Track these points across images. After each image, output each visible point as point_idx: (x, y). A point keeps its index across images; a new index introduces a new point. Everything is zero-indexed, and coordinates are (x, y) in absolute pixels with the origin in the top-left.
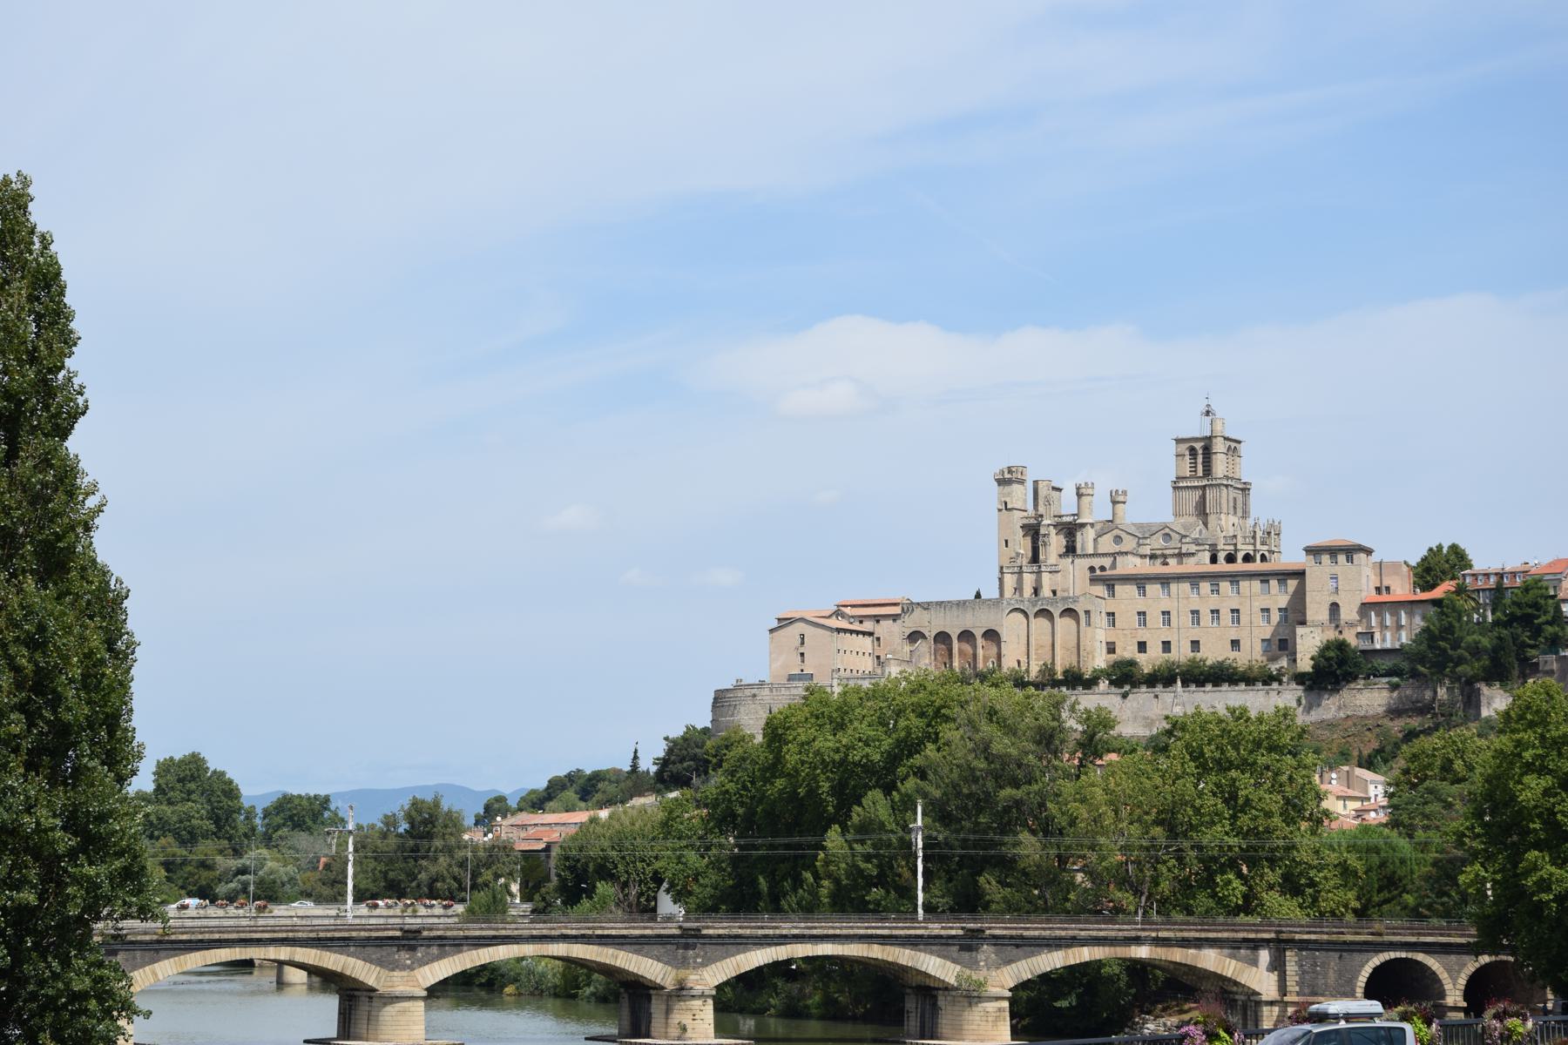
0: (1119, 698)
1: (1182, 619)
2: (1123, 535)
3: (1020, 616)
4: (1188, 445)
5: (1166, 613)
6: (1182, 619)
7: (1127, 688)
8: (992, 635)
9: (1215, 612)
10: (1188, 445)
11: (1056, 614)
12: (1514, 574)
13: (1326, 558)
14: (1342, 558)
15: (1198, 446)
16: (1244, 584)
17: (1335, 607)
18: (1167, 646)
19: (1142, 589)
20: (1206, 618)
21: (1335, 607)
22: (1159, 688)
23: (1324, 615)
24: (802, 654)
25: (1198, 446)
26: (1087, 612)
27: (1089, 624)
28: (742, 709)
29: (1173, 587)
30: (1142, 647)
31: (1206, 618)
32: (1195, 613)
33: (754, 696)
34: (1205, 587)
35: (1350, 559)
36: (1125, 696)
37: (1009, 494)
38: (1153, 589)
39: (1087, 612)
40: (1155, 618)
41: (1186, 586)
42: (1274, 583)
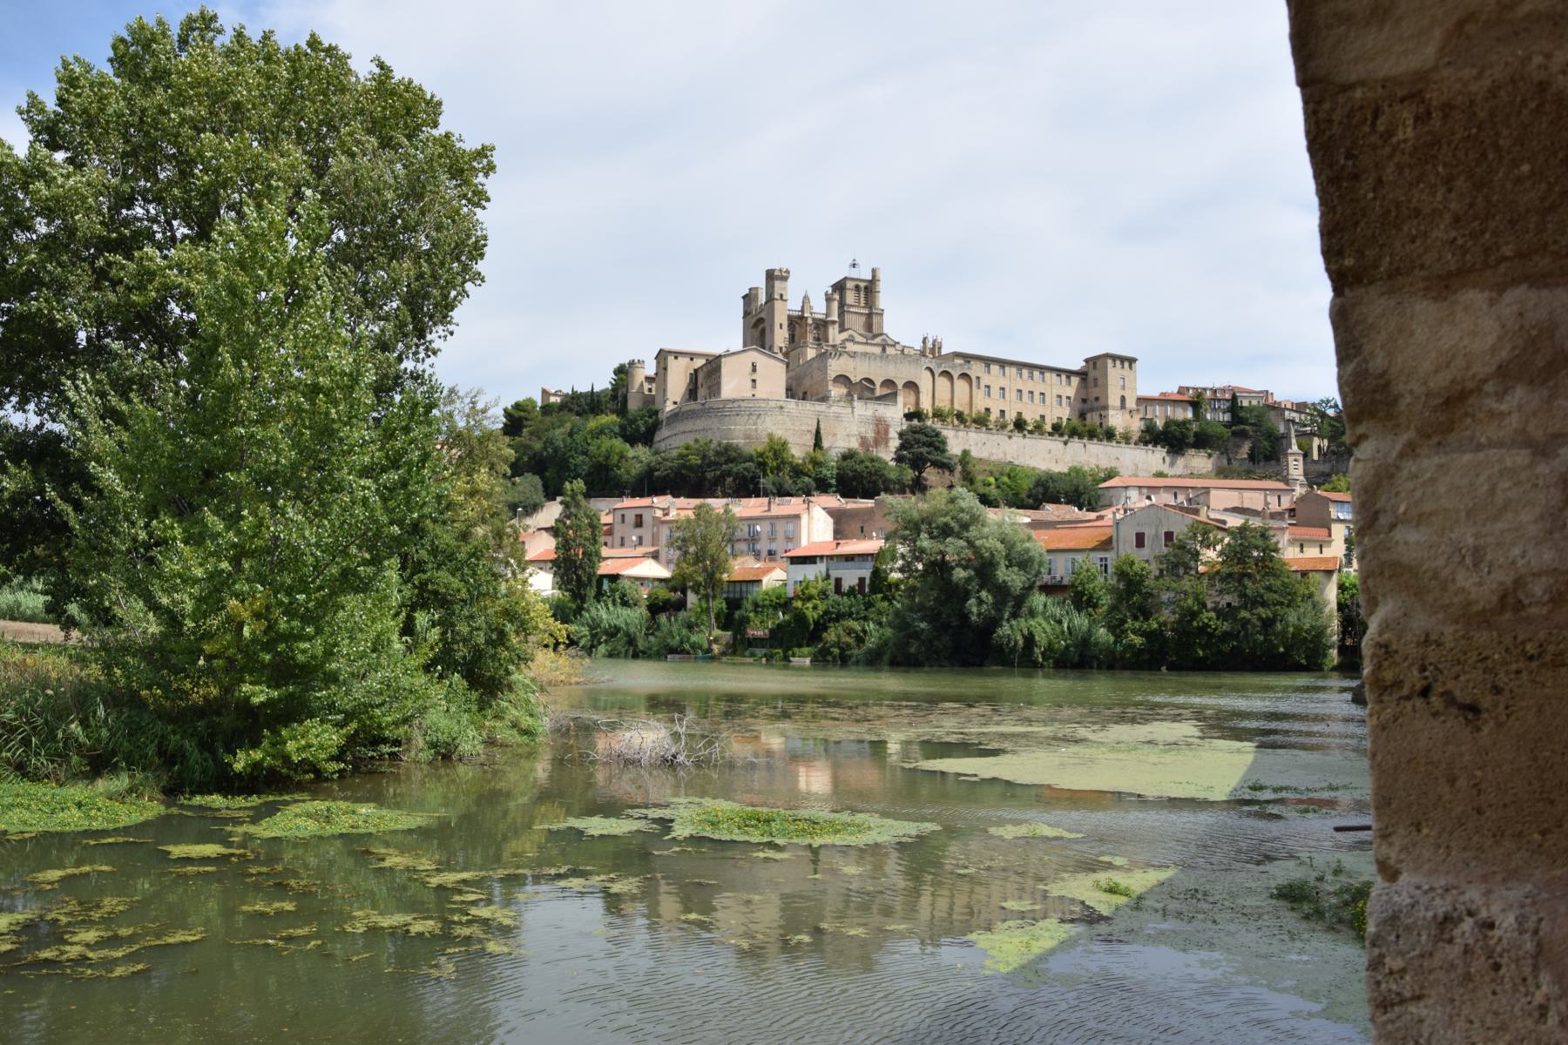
0: (1062, 445)
1: (1011, 395)
2: (855, 335)
3: (929, 373)
4: (855, 283)
5: (1003, 389)
6: (1011, 395)
7: (1066, 438)
8: (912, 386)
9: (1031, 393)
10: (855, 283)
11: (956, 377)
12: (1223, 390)
13: (1118, 363)
14: (1126, 364)
15: (862, 285)
16: (1047, 375)
17: (1123, 399)
18: (1003, 412)
19: (988, 366)
20: (1026, 396)
21: (1123, 399)
22: (1085, 440)
23: (1118, 403)
24: (754, 381)
25: (862, 285)
26: (978, 378)
27: (979, 388)
28: (768, 419)
29: (1007, 369)
30: (988, 410)
31: (1026, 396)
32: (1020, 391)
33: (781, 408)
34: (1025, 372)
35: (1131, 367)
36: (1066, 443)
37: (785, 289)
38: (995, 368)
39: (978, 378)
40: (995, 391)
41: (1014, 370)
42: (1064, 377)
